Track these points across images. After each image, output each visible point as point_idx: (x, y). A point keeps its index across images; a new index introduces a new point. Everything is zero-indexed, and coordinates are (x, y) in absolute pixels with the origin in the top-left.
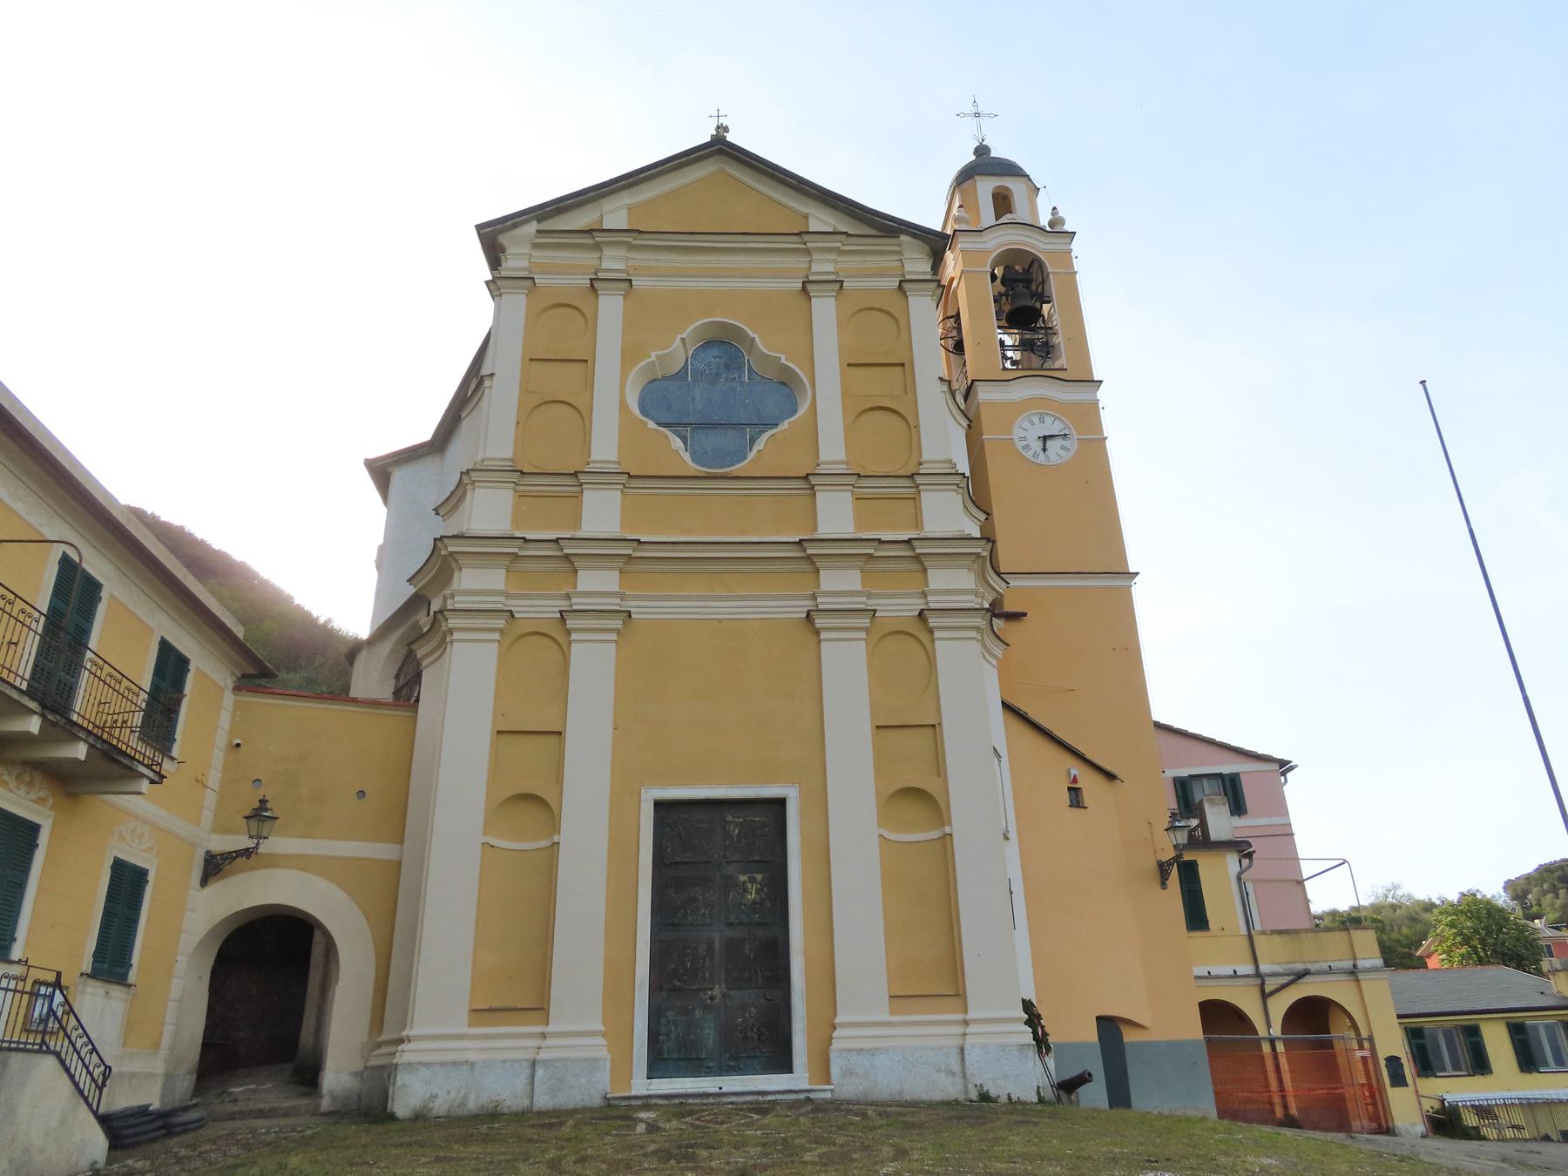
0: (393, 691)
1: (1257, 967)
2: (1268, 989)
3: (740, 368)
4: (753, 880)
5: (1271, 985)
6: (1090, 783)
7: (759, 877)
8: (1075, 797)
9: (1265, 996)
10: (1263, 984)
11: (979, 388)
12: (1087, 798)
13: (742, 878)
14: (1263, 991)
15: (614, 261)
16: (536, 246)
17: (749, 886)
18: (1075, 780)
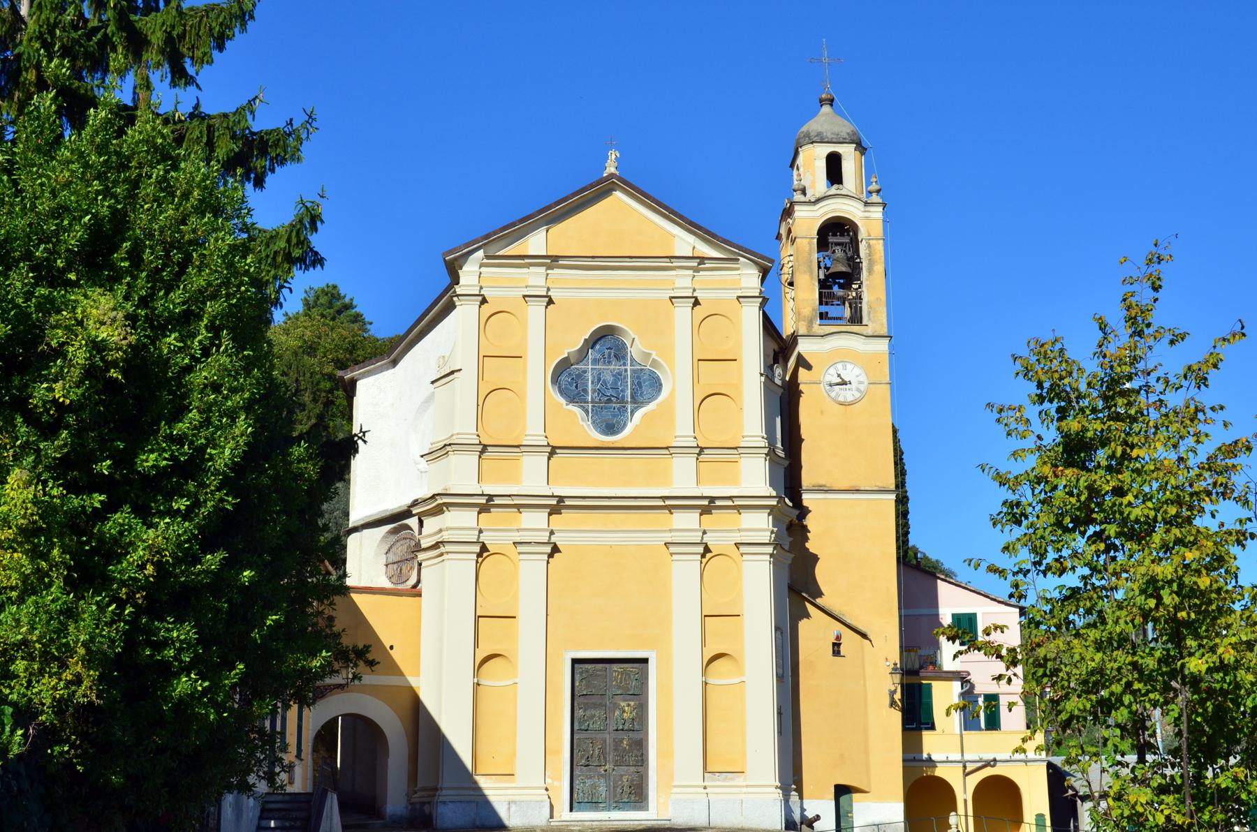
0: (385, 563)
1: (962, 755)
2: (968, 769)
3: (624, 357)
4: (629, 705)
5: (970, 767)
6: (849, 638)
7: (632, 703)
8: (836, 648)
9: (966, 774)
10: (965, 767)
11: (799, 341)
12: (843, 649)
13: (623, 704)
14: (964, 771)
15: (535, 278)
16: (482, 265)
17: (626, 708)
18: (838, 638)
